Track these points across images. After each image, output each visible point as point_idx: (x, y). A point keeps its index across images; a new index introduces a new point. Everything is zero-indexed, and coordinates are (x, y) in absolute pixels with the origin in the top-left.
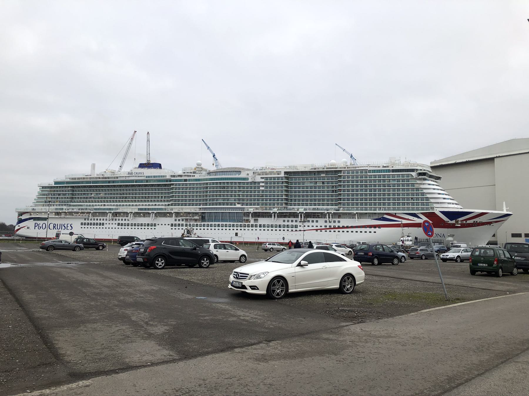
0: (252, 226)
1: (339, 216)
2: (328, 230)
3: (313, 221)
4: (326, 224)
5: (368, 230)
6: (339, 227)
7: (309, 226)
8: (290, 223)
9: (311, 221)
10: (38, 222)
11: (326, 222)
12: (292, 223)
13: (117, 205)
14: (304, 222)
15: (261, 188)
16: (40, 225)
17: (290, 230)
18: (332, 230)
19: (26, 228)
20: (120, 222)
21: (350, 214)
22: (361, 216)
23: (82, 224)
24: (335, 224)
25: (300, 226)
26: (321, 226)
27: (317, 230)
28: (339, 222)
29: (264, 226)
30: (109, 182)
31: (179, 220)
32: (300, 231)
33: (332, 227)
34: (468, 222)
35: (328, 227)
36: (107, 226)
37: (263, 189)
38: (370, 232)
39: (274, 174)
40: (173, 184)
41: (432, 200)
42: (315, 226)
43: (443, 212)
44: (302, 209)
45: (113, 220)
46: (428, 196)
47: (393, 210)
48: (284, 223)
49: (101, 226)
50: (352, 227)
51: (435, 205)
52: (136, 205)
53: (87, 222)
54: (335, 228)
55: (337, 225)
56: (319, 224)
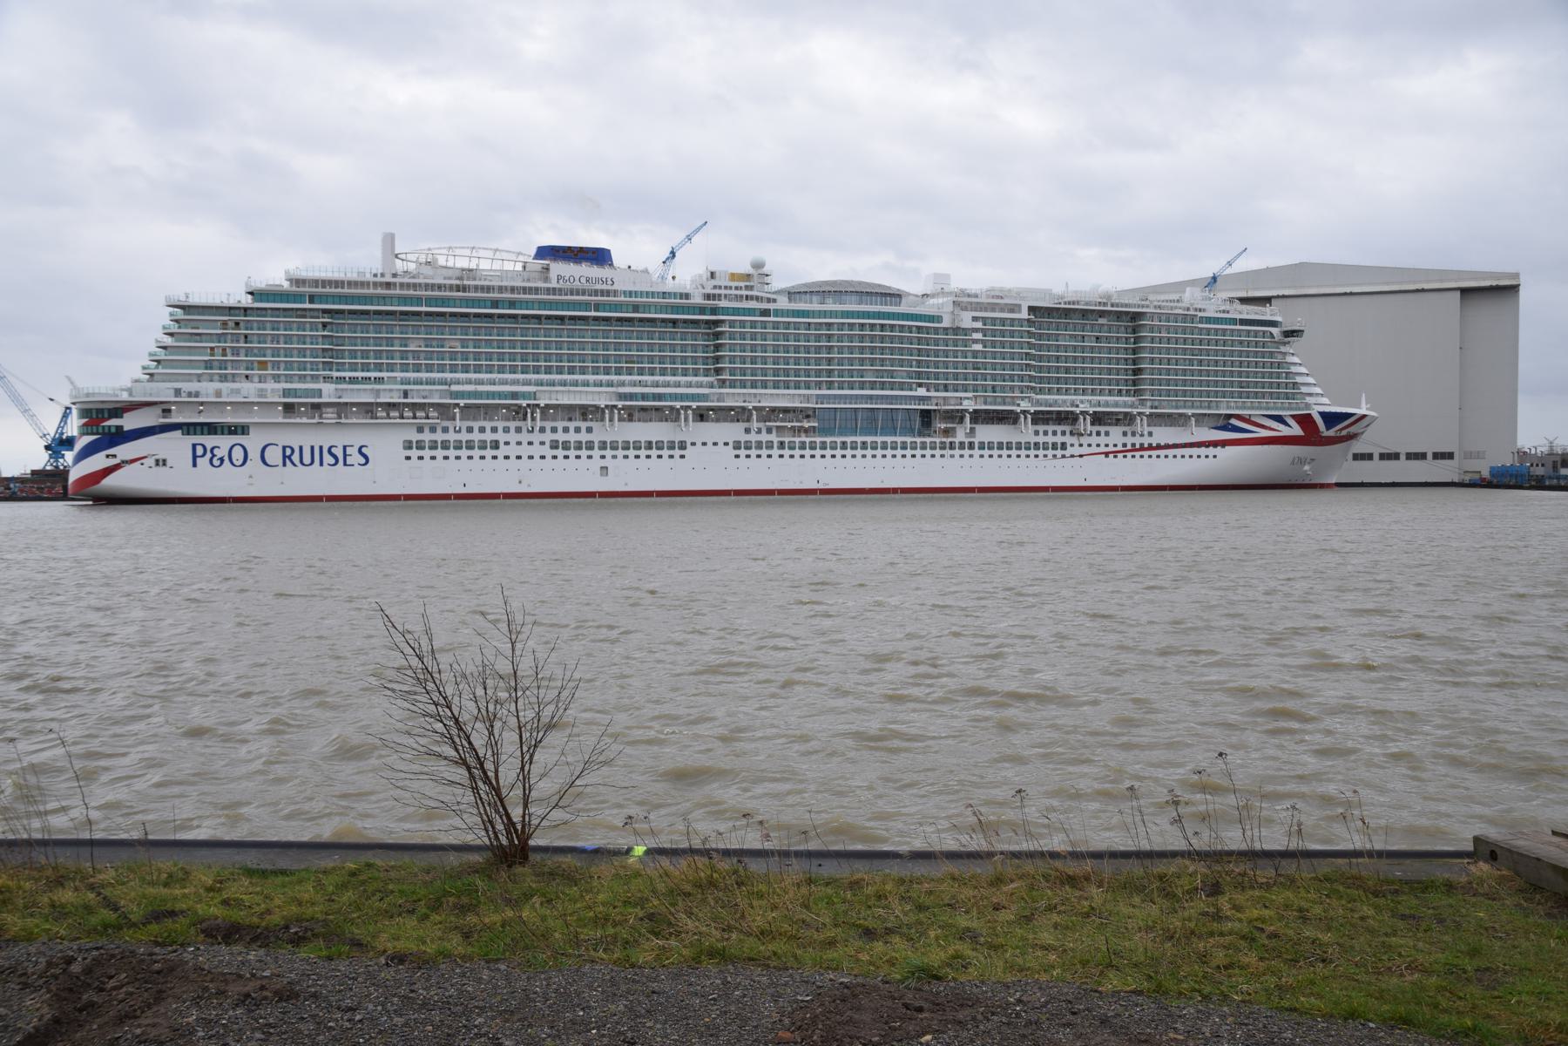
6: (1151, 448)
10: (210, 441)
16: (222, 452)
18: (1137, 454)
19: (150, 462)
20: (560, 437)
21: (1170, 415)
23: (408, 445)
27: (1107, 454)
30: (495, 304)
36: (513, 450)
37: (978, 347)
39: (1002, 310)
49: (489, 453)
51: (1309, 400)
52: (610, 384)
53: (427, 437)
56: (1110, 440)
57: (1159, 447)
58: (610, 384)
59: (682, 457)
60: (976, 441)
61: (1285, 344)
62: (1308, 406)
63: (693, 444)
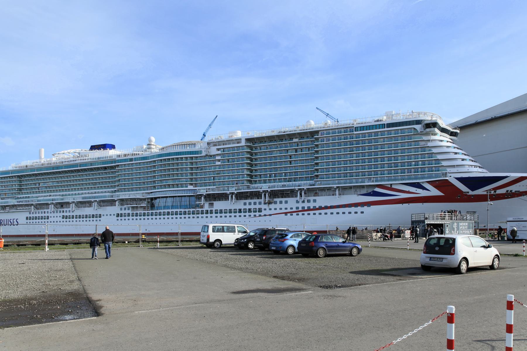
0: (207, 212)
2: (300, 213)
3: (281, 202)
4: (298, 205)
5: (353, 209)
6: (315, 209)
7: (275, 209)
8: (252, 207)
9: (278, 202)
11: (298, 202)
12: (255, 207)
13: (63, 195)
14: (270, 203)
15: (218, 163)
17: (252, 216)
18: (306, 213)
20: (65, 214)
22: (344, 190)
25: (265, 209)
26: (292, 208)
27: (286, 214)
28: (315, 201)
29: (221, 212)
31: (125, 209)
32: (265, 215)
33: (306, 208)
35: (300, 209)
37: (219, 163)
38: (356, 213)
39: (233, 143)
40: (118, 166)
41: (444, 163)
42: (283, 209)
43: (460, 180)
44: (265, 187)
45: (54, 212)
47: (388, 180)
48: (245, 207)
51: (449, 170)
53: (31, 215)
54: (309, 209)
55: (312, 205)
56: (288, 206)
57: (321, 208)
58: (79, 194)
59: (100, 220)
60: (214, 209)
61: (427, 134)
62: (445, 174)
63: (103, 215)
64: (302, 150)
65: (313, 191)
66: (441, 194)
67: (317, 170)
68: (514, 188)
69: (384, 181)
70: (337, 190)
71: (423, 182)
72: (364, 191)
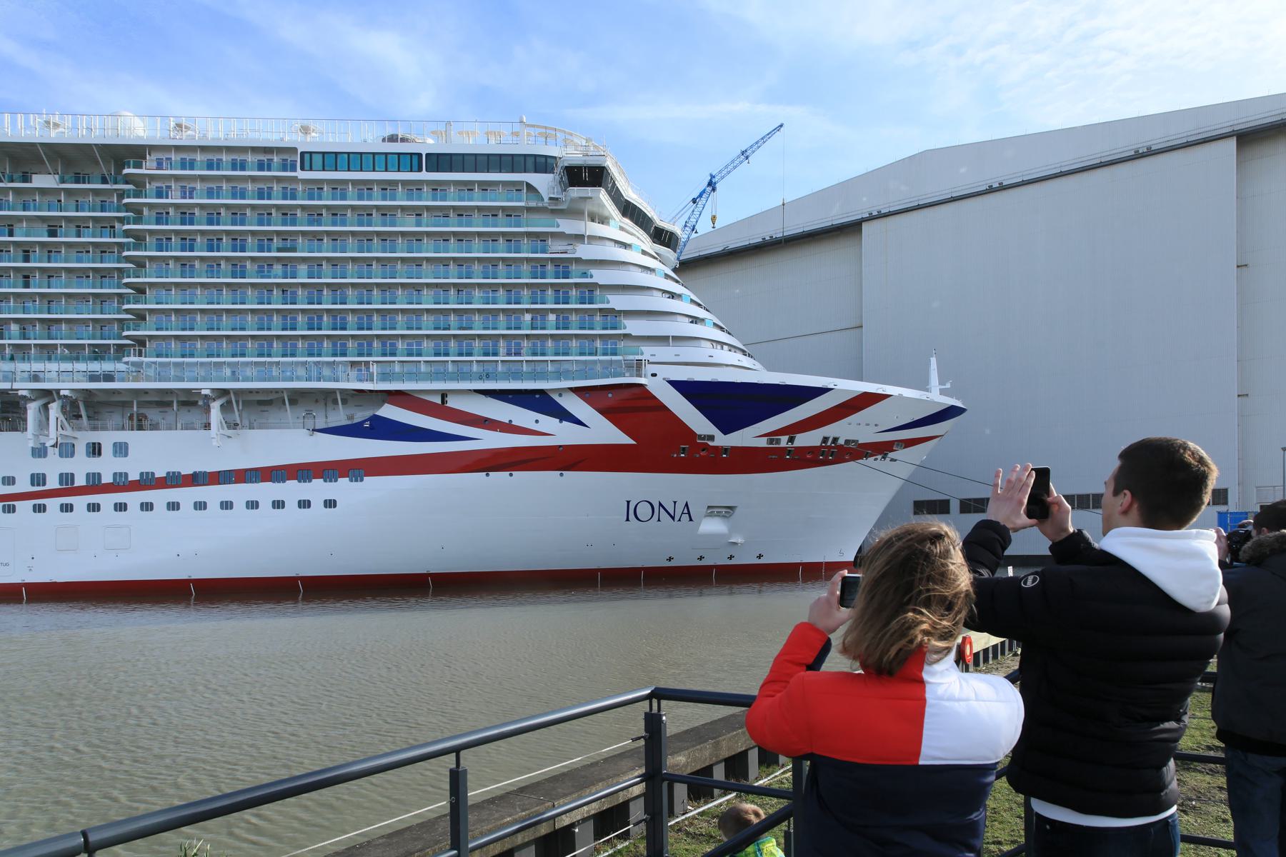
1: (144, 409)
4: (39, 466)
5: (291, 490)
22: (254, 406)
24: (94, 465)
28: (121, 450)
33: (80, 481)
34: (803, 440)
38: (305, 504)
43: (687, 389)
46: (617, 302)
47: (431, 377)
50: (241, 476)
51: (648, 352)
54: (95, 486)
55: (107, 467)
62: (638, 367)
64: (79, 226)
65: (125, 405)
66: (623, 439)
67: (140, 316)
68: (842, 431)
69: (416, 376)
70: (215, 407)
71: (560, 392)
72: (340, 417)
